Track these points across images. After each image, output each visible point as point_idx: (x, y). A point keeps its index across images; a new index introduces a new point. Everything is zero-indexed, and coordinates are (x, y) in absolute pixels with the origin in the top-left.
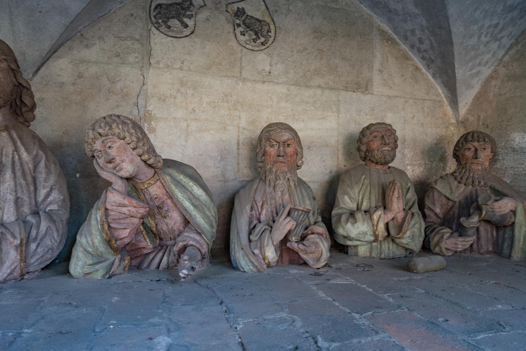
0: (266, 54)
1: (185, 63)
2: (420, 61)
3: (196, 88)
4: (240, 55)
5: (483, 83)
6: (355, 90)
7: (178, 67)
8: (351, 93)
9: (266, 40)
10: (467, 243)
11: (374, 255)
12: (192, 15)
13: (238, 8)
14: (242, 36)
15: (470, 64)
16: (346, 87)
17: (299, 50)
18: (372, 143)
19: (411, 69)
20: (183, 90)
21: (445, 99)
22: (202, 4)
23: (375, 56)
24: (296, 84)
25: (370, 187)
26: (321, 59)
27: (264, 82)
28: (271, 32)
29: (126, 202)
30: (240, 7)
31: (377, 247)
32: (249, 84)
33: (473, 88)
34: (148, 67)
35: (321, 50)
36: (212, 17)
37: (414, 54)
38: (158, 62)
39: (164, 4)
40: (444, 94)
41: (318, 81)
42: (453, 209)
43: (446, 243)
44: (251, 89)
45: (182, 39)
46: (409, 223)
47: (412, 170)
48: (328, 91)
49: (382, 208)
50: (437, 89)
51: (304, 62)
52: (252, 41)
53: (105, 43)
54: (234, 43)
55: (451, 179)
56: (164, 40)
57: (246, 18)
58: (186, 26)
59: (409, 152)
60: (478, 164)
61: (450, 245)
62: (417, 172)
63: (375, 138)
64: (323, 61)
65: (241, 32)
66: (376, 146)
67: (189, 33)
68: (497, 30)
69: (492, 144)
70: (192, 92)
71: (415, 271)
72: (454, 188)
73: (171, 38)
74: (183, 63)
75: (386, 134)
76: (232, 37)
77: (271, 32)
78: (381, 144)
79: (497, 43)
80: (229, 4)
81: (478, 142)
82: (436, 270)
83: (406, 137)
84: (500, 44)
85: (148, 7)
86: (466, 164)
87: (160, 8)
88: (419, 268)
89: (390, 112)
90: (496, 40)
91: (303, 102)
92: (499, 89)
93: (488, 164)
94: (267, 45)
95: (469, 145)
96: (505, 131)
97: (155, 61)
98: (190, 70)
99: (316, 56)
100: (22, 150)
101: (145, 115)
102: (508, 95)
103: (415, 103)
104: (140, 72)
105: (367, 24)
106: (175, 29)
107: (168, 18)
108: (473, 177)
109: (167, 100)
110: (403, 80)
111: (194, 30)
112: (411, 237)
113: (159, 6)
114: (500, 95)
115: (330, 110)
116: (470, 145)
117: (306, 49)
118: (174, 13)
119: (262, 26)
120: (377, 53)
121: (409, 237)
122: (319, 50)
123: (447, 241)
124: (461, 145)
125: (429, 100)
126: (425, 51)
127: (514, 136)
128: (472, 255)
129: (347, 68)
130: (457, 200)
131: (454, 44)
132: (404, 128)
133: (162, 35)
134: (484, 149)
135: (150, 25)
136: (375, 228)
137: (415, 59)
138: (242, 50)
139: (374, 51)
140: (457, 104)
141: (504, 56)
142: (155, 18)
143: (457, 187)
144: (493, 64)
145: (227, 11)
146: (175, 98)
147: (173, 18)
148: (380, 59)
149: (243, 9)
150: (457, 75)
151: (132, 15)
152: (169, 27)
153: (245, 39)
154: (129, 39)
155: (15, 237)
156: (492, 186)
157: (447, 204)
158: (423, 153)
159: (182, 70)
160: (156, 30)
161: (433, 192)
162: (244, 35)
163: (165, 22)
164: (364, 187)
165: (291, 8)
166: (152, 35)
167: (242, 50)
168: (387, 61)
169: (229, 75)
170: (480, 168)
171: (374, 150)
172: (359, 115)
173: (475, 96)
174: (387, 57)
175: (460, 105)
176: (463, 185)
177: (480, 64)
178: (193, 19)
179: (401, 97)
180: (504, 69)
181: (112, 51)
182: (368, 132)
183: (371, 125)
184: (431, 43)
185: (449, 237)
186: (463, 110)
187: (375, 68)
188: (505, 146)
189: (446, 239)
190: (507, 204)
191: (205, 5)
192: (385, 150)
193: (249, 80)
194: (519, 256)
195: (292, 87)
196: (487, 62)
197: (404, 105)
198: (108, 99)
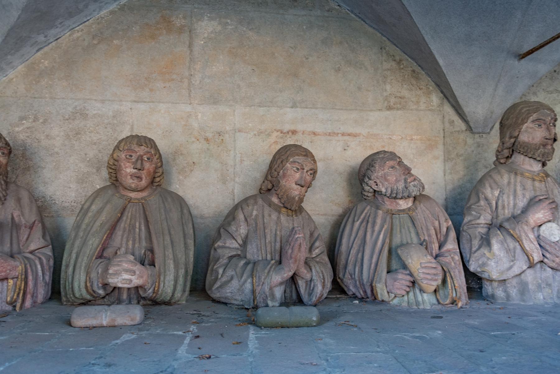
53: (537, 97)
151: (555, 71)
154: (555, 92)
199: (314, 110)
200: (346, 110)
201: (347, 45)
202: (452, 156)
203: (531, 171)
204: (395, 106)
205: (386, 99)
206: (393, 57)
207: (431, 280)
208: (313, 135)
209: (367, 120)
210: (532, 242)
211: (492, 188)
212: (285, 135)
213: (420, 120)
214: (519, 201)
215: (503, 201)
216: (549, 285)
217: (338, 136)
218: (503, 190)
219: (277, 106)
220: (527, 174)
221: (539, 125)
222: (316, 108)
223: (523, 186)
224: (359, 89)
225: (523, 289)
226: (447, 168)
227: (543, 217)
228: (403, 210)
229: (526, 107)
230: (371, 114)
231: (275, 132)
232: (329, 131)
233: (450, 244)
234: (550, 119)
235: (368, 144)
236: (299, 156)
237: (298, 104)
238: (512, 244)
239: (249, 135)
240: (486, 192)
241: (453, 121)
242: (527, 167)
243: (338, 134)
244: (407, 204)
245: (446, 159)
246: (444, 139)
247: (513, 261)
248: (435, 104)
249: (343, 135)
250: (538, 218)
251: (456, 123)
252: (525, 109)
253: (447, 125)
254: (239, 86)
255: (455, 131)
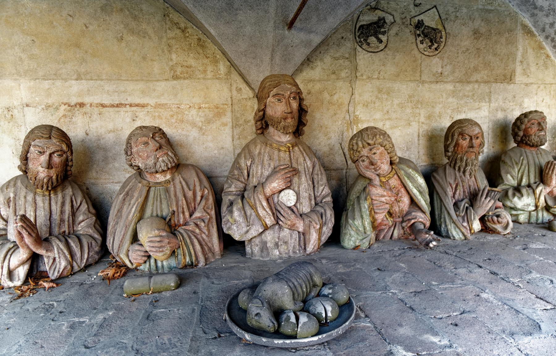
0: (439, 58)
1: (381, 73)
2: (550, 50)
3: (389, 93)
4: (420, 61)
7: (376, 77)
8: (499, 84)
9: (438, 46)
12: (385, 31)
13: (418, 20)
14: (421, 45)
16: (496, 79)
17: (463, 51)
19: (543, 57)
20: (380, 96)
22: (393, 21)
24: (461, 82)
26: (479, 56)
27: (437, 82)
28: (442, 38)
29: (385, 194)
30: (420, 20)
32: (426, 85)
34: (355, 80)
35: (479, 49)
36: (400, 31)
38: (362, 75)
39: (364, 25)
41: (476, 76)
44: (428, 89)
45: (379, 53)
48: (482, 84)
51: (466, 61)
52: (428, 48)
54: (416, 52)
56: (366, 56)
57: (425, 28)
58: (381, 41)
64: (480, 59)
65: (421, 41)
67: (383, 47)
70: (386, 97)
73: (371, 54)
74: (379, 73)
76: (414, 46)
77: (442, 38)
80: (412, 18)
85: (354, 29)
87: (362, 29)
91: (465, 96)
94: (439, 50)
97: (360, 74)
98: (384, 79)
99: (475, 54)
100: (307, 159)
101: (354, 119)
103: (545, 87)
104: (349, 85)
105: (513, 20)
106: (373, 45)
107: (368, 37)
109: (369, 105)
111: (387, 44)
113: (362, 27)
115: (484, 101)
117: (468, 50)
118: (372, 31)
119: (436, 34)
120: (520, 46)
122: (477, 49)
129: (497, 63)
133: (364, 52)
135: (356, 44)
138: (421, 57)
142: (359, 38)
145: (411, 24)
146: (374, 103)
147: (371, 36)
149: (422, 20)
152: (368, 44)
153: (423, 47)
154: (341, 58)
155: (316, 224)
159: (379, 79)
160: (360, 48)
162: (423, 43)
163: (365, 40)
165: (458, 14)
166: (357, 53)
167: (421, 57)
168: (527, 52)
169: (412, 79)
172: (504, 102)
178: (386, 35)
179: (535, 84)
181: (330, 70)
191: (395, 21)
193: (426, 82)
195: (457, 84)
198: (328, 109)
199: (99, 82)
200: (131, 80)
201: (128, 13)
202: (240, 122)
203: (279, 142)
204: (182, 76)
205: (172, 68)
206: (177, 25)
207: (156, 252)
208: (101, 107)
209: (154, 90)
210: (265, 209)
211: (245, 158)
212: (73, 108)
213: (207, 88)
214: (265, 170)
215: (253, 171)
216: (286, 243)
217: (125, 107)
218: (254, 159)
219: (62, 79)
220: (275, 145)
221: (279, 100)
222: (102, 80)
223: (270, 156)
224: (144, 58)
225: (264, 247)
226: (235, 134)
227: (277, 186)
228: (160, 183)
229: (270, 82)
230: (158, 84)
231: (63, 105)
232: (116, 103)
233: (199, 212)
234: (289, 93)
235: (157, 114)
236: (40, 139)
237: (83, 76)
238: (249, 211)
239: (37, 109)
240: (240, 162)
241: (241, 89)
242: (277, 138)
243: (126, 105)
244: (165, 177)
245: (234, 125)
246: (232, 107)
247: (248, 226)
248: (222, 72)
249: (131, 106)
250: (274, 187)
251: (244, 90)
252: (268, 84)
253: (235, 93)
254: (21, 59)
255: (242, 99)
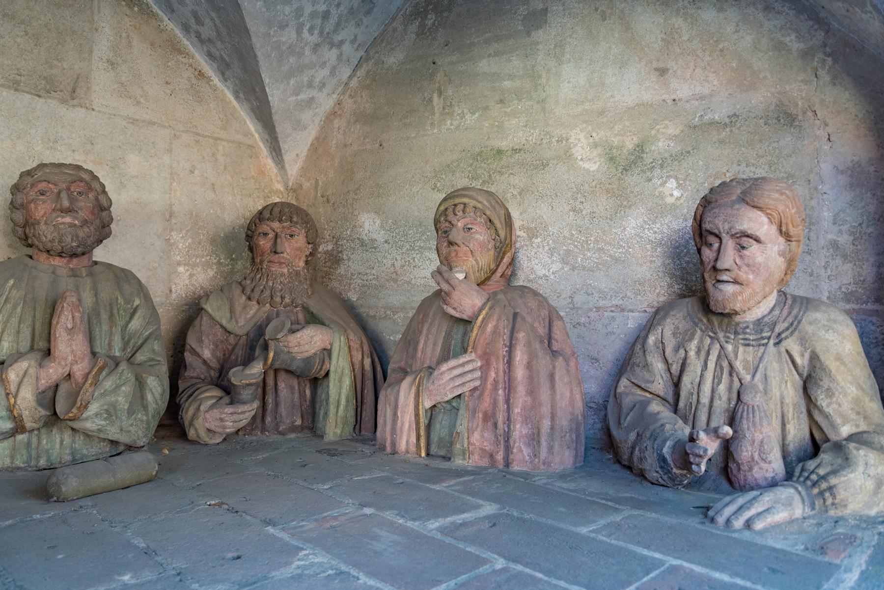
5: (322, 123)
6: (42, 93)
10: (241, 416)
11: (19, 463)
15: (292, 82)
18: (32, 205)
19: (186, 74)
21: (261, 145)
23: (96, 30)
25: (23, 308)
31: (29, 444)
33: (305, 128)
37: (194, 46)
40: (259, 134)
42: (236, 351)
43: (205, 419)
46: (96, 383)
47: (188, 274)
49: (38, 355)
50: (245, 123)
55: (237, 291)
59: (182, 237)
60: (281, 263)
61: (213, 423)
62: (200, 280)
63: (42, 194)
66: (42, 213)
68: (329, 26)
69: (306, 227)
71: (55, 498)
72: (238, 308)
75: (72, 189)
78: (54, 210)
79: (334, 52)
81: (280, 221)
82: (127, 483)
83: (176, 209)
84: (341, 54)
86: (261, 262)
88: (64, 489)
89: (137, 152)
90: (332, 45)
92: (344, 135)
93: (302, 264)
95: (265, 228)
96: (351, 211)
102: (355, 147)
103: (197, 142)
108: (273, 287)
110: (168, 92)
112: (105, 416)
114: (345, 146)
116: (265, 227)
121: (96, 415)
123: (207, 416)
124: (254, 227)
125: (229, 141)
126: (210, 40)
127: (363, 219)
128: (264, 437)
130: (240, 332)
131: (252, 34)
132: (170, 190)
134: (291, 236)
136: (12, 401)
137: (197, 56)
139: (96, 19)
140: (281, 155)
141: (350, 77)
143: (245, 308)
144: (336, 89)
148: (112, 38)
150: (270, 98)
156: (305, 305)
157: (227, 340)
158: (213, 241)
161: (202, 317)
164: (9, 306)
168: (130, 45)
170: (285, 271)
171: (38, 223)
173: (312, 145)
174: (128, 36)
175: (286, 158)
176: (255, 303)
177: (310, 85)
179: (164, 127)
180: (350, 101)
182: (29, 180)
183: (42, 166)
184: (215, 25)
185: (212, 407)
186: (293, 169)
187: (96, 54)
188: (350, 236)
189: (206, 412)
190: (312, 337)
192: (63, 223)
194: (339, 431)
196: (323, 85)
197: (171, 143)
